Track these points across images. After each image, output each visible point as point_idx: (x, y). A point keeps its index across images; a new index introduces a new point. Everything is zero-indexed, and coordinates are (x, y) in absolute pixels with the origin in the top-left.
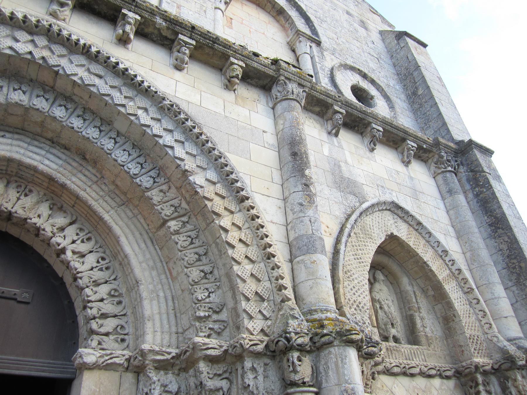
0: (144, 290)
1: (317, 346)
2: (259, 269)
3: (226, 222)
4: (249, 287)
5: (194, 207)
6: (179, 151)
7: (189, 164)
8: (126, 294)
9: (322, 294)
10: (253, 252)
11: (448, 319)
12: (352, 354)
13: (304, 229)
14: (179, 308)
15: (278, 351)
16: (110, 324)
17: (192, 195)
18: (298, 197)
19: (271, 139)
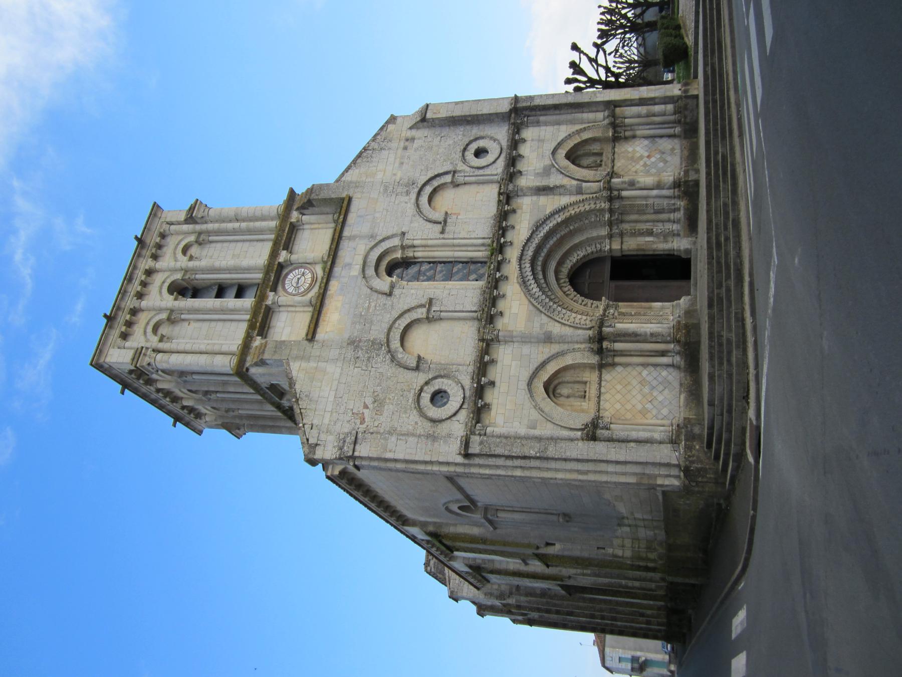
0: (589, 236)
1: (610, 189)
2: (586, 204)
3: (573, 212)
4: (593, 206)
5: (566, 222)
6: (551, 225)
7: (555, 222)
8: (589, 241)
9: (595, 186)
10: (581, 205)
11: (594, 140)
12: (613, 180)
13: (574, 189)
14: (593, 225)
15: (610, 199)
16: (598, 246)
17: (563, 222)
18: (562, 190)
19: (535, 198)
